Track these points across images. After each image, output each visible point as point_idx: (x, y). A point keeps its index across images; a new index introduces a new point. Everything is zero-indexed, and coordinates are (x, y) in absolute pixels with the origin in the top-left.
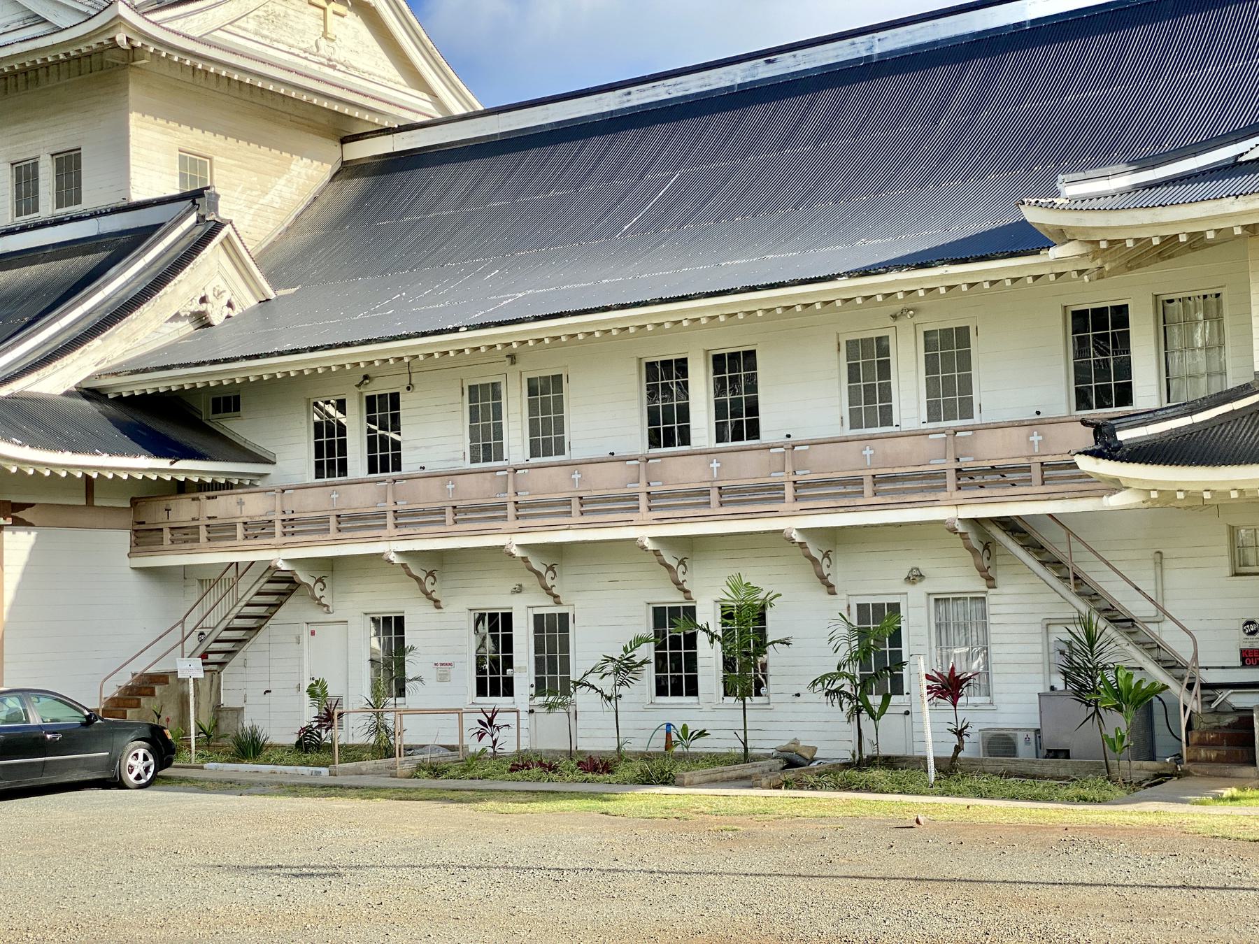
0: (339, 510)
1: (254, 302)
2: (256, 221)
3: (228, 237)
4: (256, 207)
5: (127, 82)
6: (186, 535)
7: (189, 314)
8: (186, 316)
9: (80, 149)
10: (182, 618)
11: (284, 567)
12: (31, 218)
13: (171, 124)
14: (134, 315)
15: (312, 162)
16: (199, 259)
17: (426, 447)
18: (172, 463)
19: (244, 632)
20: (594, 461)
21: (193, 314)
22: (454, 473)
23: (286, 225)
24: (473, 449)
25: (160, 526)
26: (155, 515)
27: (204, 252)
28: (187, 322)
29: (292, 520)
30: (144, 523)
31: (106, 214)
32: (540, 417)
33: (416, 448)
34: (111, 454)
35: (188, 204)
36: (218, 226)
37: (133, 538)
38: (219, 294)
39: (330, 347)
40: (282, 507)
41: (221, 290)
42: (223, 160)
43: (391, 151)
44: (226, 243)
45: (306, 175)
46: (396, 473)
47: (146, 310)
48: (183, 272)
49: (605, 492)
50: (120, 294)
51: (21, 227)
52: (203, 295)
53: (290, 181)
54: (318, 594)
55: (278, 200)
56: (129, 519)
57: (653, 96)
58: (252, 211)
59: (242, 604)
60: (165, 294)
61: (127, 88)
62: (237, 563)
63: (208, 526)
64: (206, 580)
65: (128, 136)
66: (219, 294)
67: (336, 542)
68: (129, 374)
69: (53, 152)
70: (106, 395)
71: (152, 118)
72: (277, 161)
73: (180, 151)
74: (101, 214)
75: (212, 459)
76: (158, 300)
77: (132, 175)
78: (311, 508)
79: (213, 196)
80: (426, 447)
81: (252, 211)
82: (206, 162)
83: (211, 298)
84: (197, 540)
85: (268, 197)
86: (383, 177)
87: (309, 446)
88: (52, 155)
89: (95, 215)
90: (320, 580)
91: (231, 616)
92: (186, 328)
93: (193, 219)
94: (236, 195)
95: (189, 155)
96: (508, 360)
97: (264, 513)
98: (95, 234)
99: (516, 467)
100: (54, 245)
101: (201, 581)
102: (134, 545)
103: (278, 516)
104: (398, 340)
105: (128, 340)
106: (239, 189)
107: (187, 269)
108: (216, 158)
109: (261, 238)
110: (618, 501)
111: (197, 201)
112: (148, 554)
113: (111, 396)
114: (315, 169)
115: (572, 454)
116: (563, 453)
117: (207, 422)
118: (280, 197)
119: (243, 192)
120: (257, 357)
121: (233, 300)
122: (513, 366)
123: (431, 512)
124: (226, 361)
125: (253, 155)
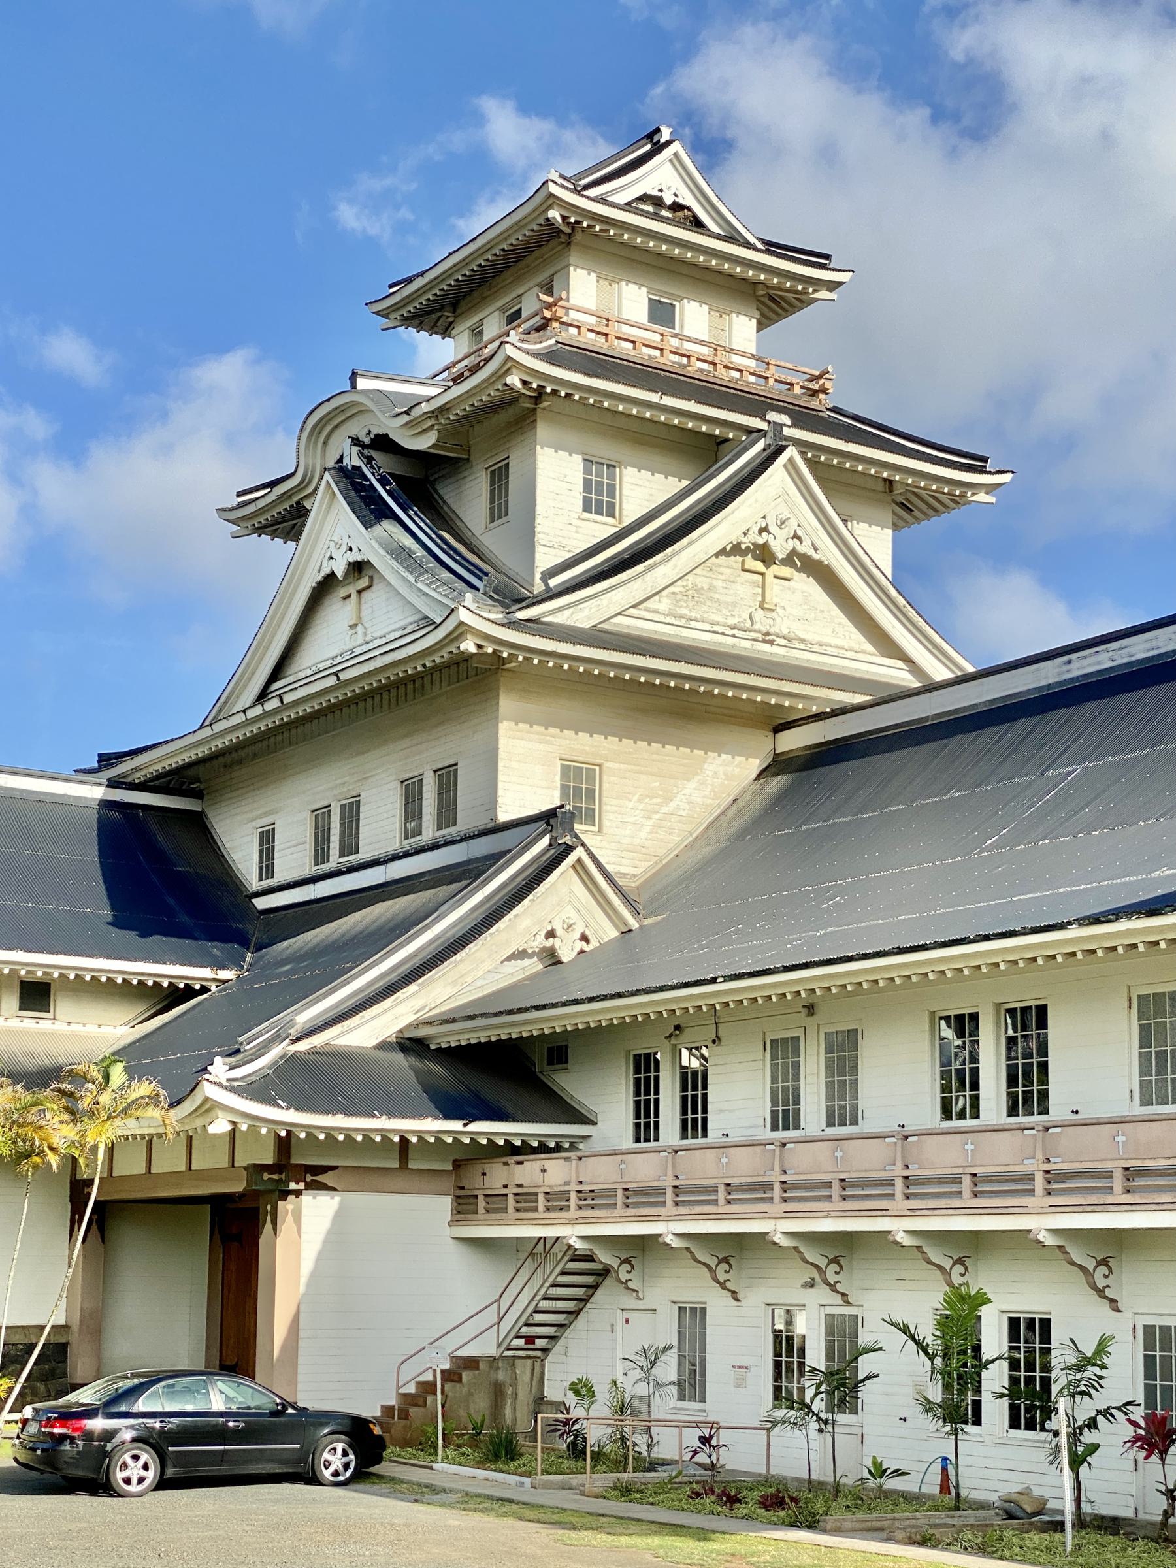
0: (625, 1182)
1: (614, 933)
2: (657, 833)
3: (579, 861)
4: (657, 816)
5: (498, 689)
6: (496, 1203)
7: (537, 950)
8: (534, 952)
9: (456, 764)
10: (497, 1297)
11: (578, 1244)
13: (551, 730)
14: (458, 957)
15: (733, 758)
16: (541, 889)
17: (730, 1111)
18: (465, 1125)
19: (565, 1315)
20: (854, 1136)
21: (544, 949)
22: (725, 1145)
23: (694, 836)
24: (774, 1114)
27: (547, 881)
28: (535, 959)
29: (592, 1191)
30: (463, 1188)
31: (474, 837)
32: (836, 1079)
33: (721, 1111)
34: (391, 1115)
35: (542, 825)
36: (569, 849)
37: (456, 1205)
38: (569, 926)
39: (605, 998)
40: (577, 1177)
41: (571, 922)
42: (617, 765)
43: (823, 741)
44: (578, 867)
45: (726, 774)
46: (656, 1144)
47: (473, 950)
48: (520, 905)
49: (863, 1175)
50: (449, 935)
51: (404, 852)
52: (549, 928)
53: (701, 784)
54: (624, 1276)
55: (687, 806)
56: (450, 1183)
57: (1094, 664)
58: (651, 822)
59: (547, 1284)
60: (497, 931)
61: (498, 695)
62: (545, 1238)
63: (516, 1194)
65: (497, 749)
66: (569, 926)
67: (620, 1220)
68: (441, 1024)
69: (435, 768)
71: (528, 726)
72: (686, 761)
73: (561, 759)
75: (515, 1120)
76: (489, 939)
77: (500, 792)
78: (601, 1180)
79: (568, 815)
80: (730, 1111)
81: (651, 822)
82: (595, 770)
83: (559, 932)
84: (505, 1210)
85: (673, 804)
86: (805, 773)
87: (627, 1104)
88: (435, 771)
89: (465, 838)
90: (627, 1261)
91: (538, 1298)
92: (533, 966)
93: (545, 841)
94: (631, 805)
95: (572, 764)
96: (806, 1010)
97: (562, 1182)
98: (465, 859)
99: (783, 1141)
102: (455, 1212)
103: (574, 1187)
104: (663, 991)
105: (454, 983)
106: (635, 798)
107: (526, 902)
108: (607, 765)
109: (661, 852)
110: (876, 1185)
111: (552, 821)
112: (464, 1223)
113: (432, 1047)
114: (737, 766)
115: (865, 1127)
116: (857, 1123)
117: (540, 1075)
118: (689, 803)
119: (640, 801)
120: (544, 1007)
121: (588, 933)
122: (810, 1018)
123: (752, 1187)
124: (544, 1007)
125: (655, 756)
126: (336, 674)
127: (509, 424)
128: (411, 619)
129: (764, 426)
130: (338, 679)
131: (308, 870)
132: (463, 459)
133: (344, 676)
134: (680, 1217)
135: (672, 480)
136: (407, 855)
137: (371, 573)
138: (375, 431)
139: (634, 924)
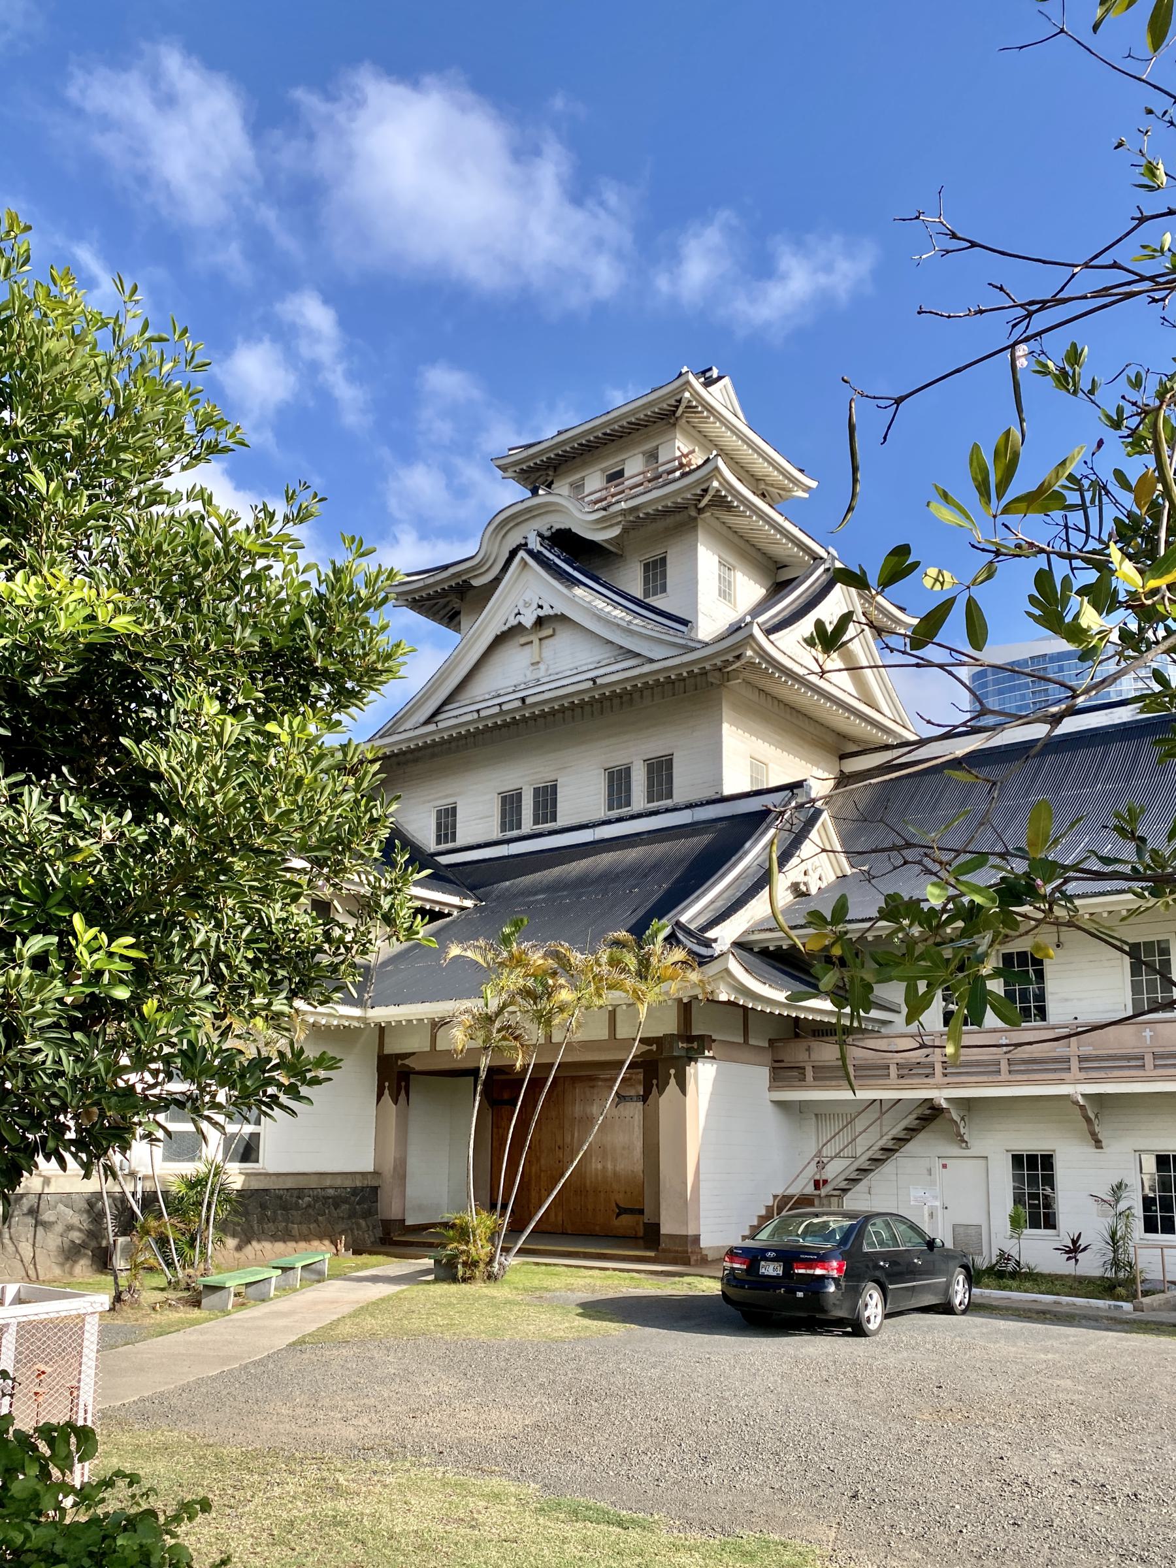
5: (721, 699)
12: (624, 811)
25: (802, 1065)
26: (796, 1053)
30: (782, 1061)
31: (702, 805)
56: (768, 1057)
64: (850, 1114)
70: (751, 949)
74: (697, 805)
83: (810, 872)
89: (690, 806)
100: (649, 832)
101: (816, 1115)
108: (771, 765)
113: (756, 950)
126: (593, 680)
127: (667, 529)
128: (606, 655)
129: (825, 555)
130: (595, 683)
131: (496, 835)
132: (616, 554)
133: (599, 681)
134: (948, 1085)
135: (758, 586)
136: (620, 820)
137: (553, 626)
138: (557, 526)
139: (849, 871)
